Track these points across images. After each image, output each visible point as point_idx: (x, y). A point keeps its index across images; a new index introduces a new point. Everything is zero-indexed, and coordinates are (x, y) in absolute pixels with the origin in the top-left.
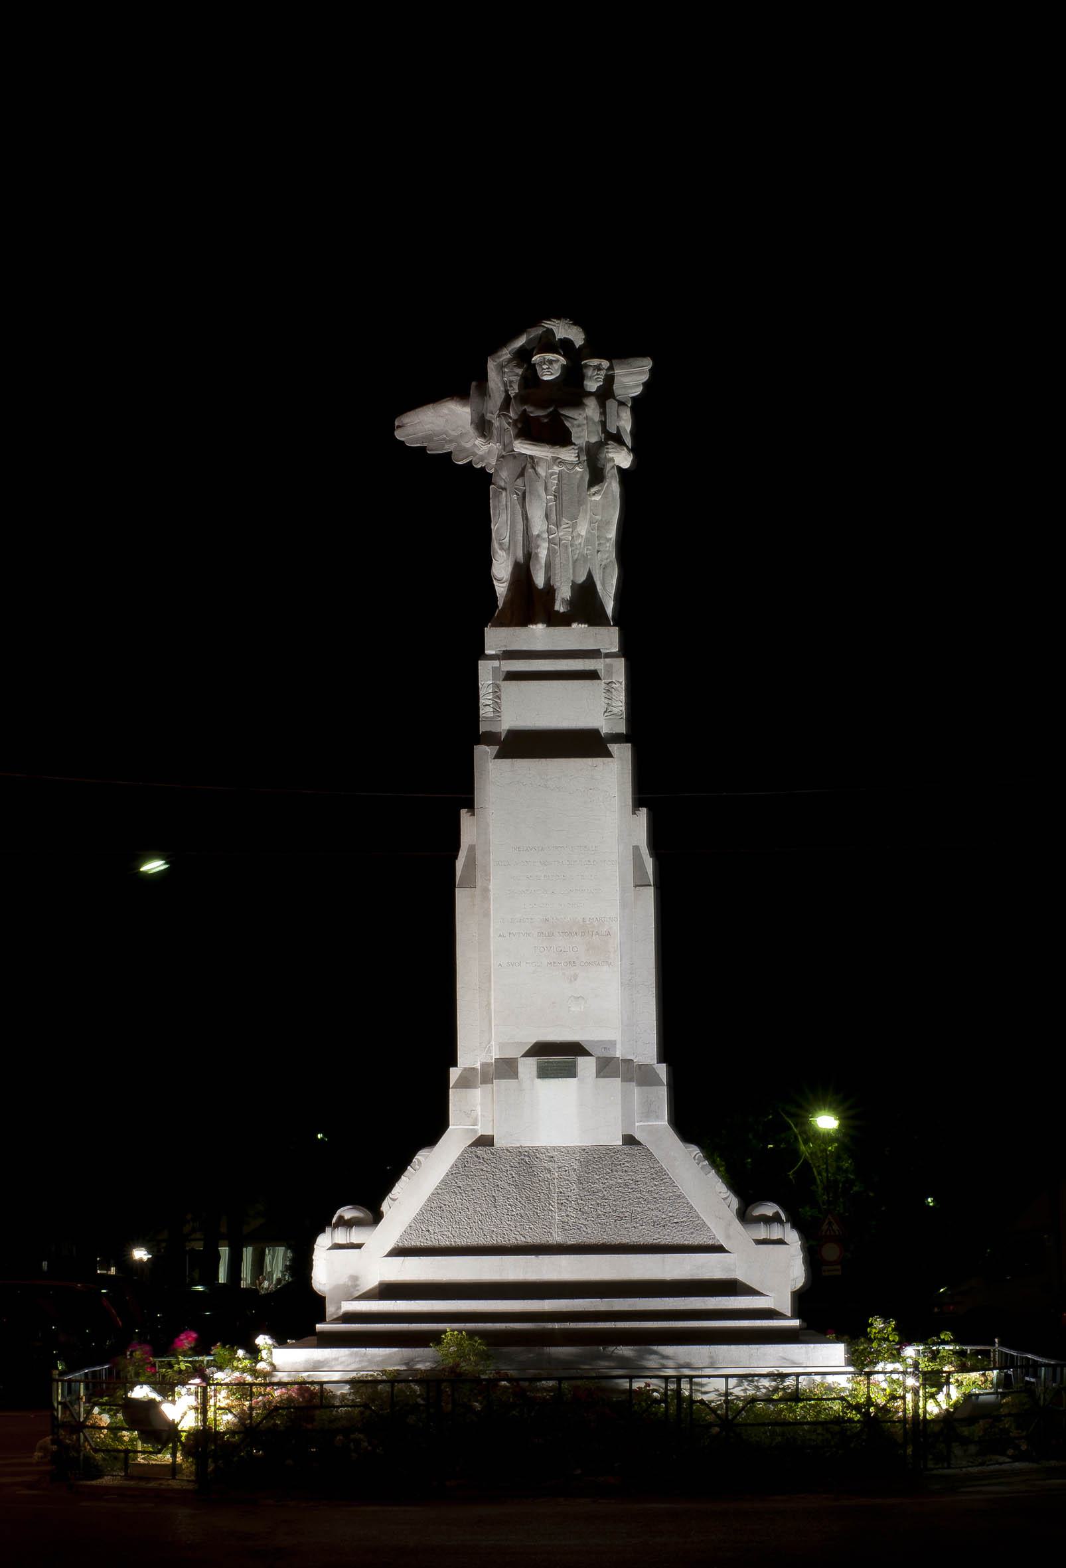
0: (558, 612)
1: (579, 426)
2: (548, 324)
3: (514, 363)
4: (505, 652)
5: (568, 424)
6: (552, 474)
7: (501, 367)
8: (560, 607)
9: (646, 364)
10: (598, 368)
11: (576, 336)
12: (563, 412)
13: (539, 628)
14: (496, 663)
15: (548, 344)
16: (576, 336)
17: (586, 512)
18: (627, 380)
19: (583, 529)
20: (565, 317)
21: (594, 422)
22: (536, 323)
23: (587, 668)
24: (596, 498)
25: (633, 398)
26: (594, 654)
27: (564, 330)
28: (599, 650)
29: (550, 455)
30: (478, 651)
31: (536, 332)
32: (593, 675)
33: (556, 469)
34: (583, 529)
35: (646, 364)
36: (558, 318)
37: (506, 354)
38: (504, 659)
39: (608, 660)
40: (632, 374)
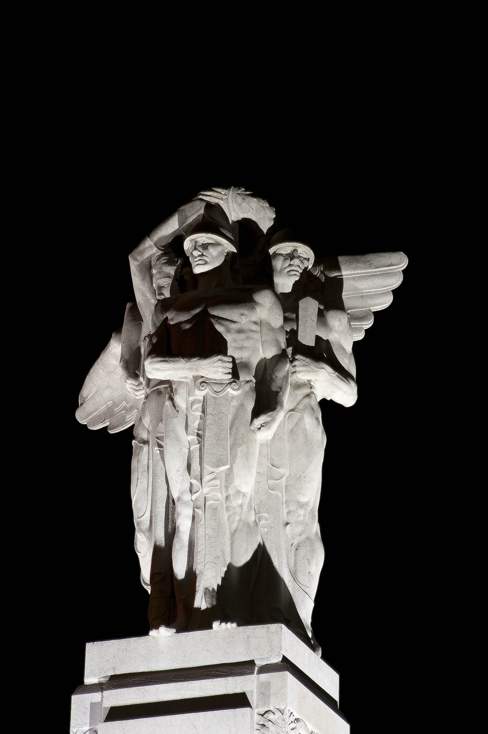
0: (199, 609)
1: (240, 331)
2: (214, 196)
3: (164, 260)
4: (113, 678)
5: (219, 328)
6: (193, 403)
7: (147, 268)
8: (201, 602)
9: (399, 262)
10: (291, 256)
11: (263, 216)
12: (215, 312)
13: (162, 635)
14: (96, 697)
15: (213, 221)
16: (263, 216)
17: (247, 456)
18: (364, 286)
19: (246, 482)
20: (238, 185)
21: (272, 329)
22: (189, 196)
23: (231, 691)
24: (268, 432)
25: (376, 314)
26: (245, 667)
27: (238, 206)
28: (251, 663)
29: (190, 375)
30: (75, 681)
31: (194, 211)
32: (239, 701)
33: (199, 394)
34: (246, 482)
35: (399, 262)
36: (226, 186)
37: (149, 248)
38: (108, 688)
39: (264, 677)
40: (374, 276)
